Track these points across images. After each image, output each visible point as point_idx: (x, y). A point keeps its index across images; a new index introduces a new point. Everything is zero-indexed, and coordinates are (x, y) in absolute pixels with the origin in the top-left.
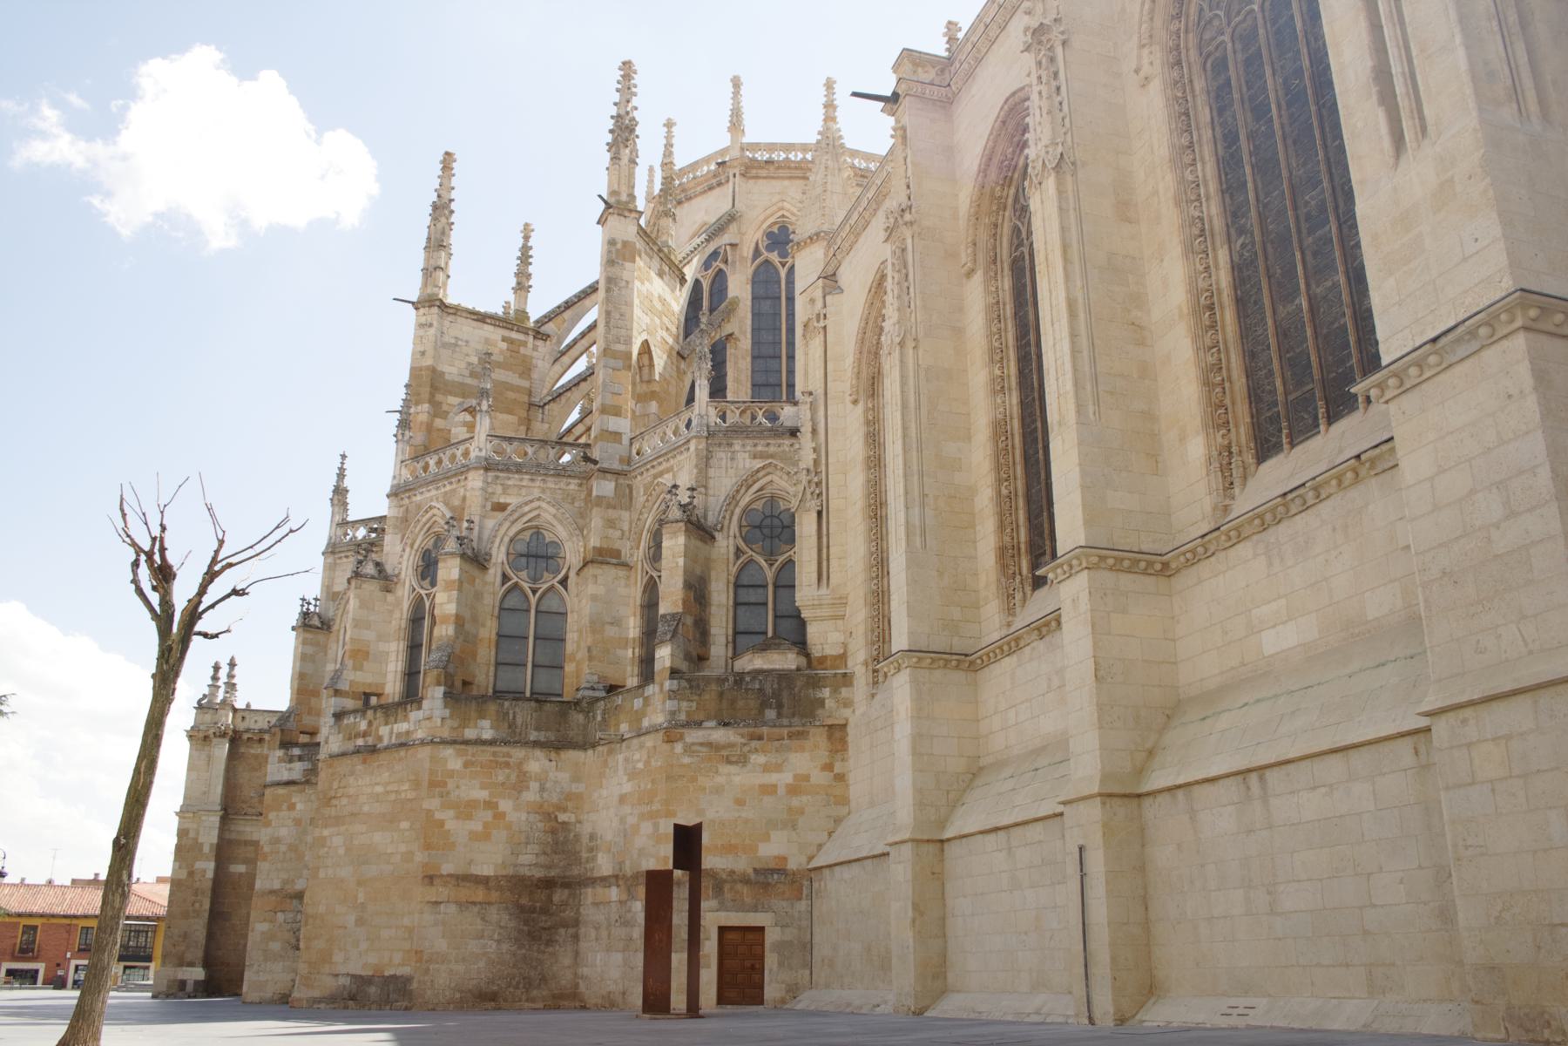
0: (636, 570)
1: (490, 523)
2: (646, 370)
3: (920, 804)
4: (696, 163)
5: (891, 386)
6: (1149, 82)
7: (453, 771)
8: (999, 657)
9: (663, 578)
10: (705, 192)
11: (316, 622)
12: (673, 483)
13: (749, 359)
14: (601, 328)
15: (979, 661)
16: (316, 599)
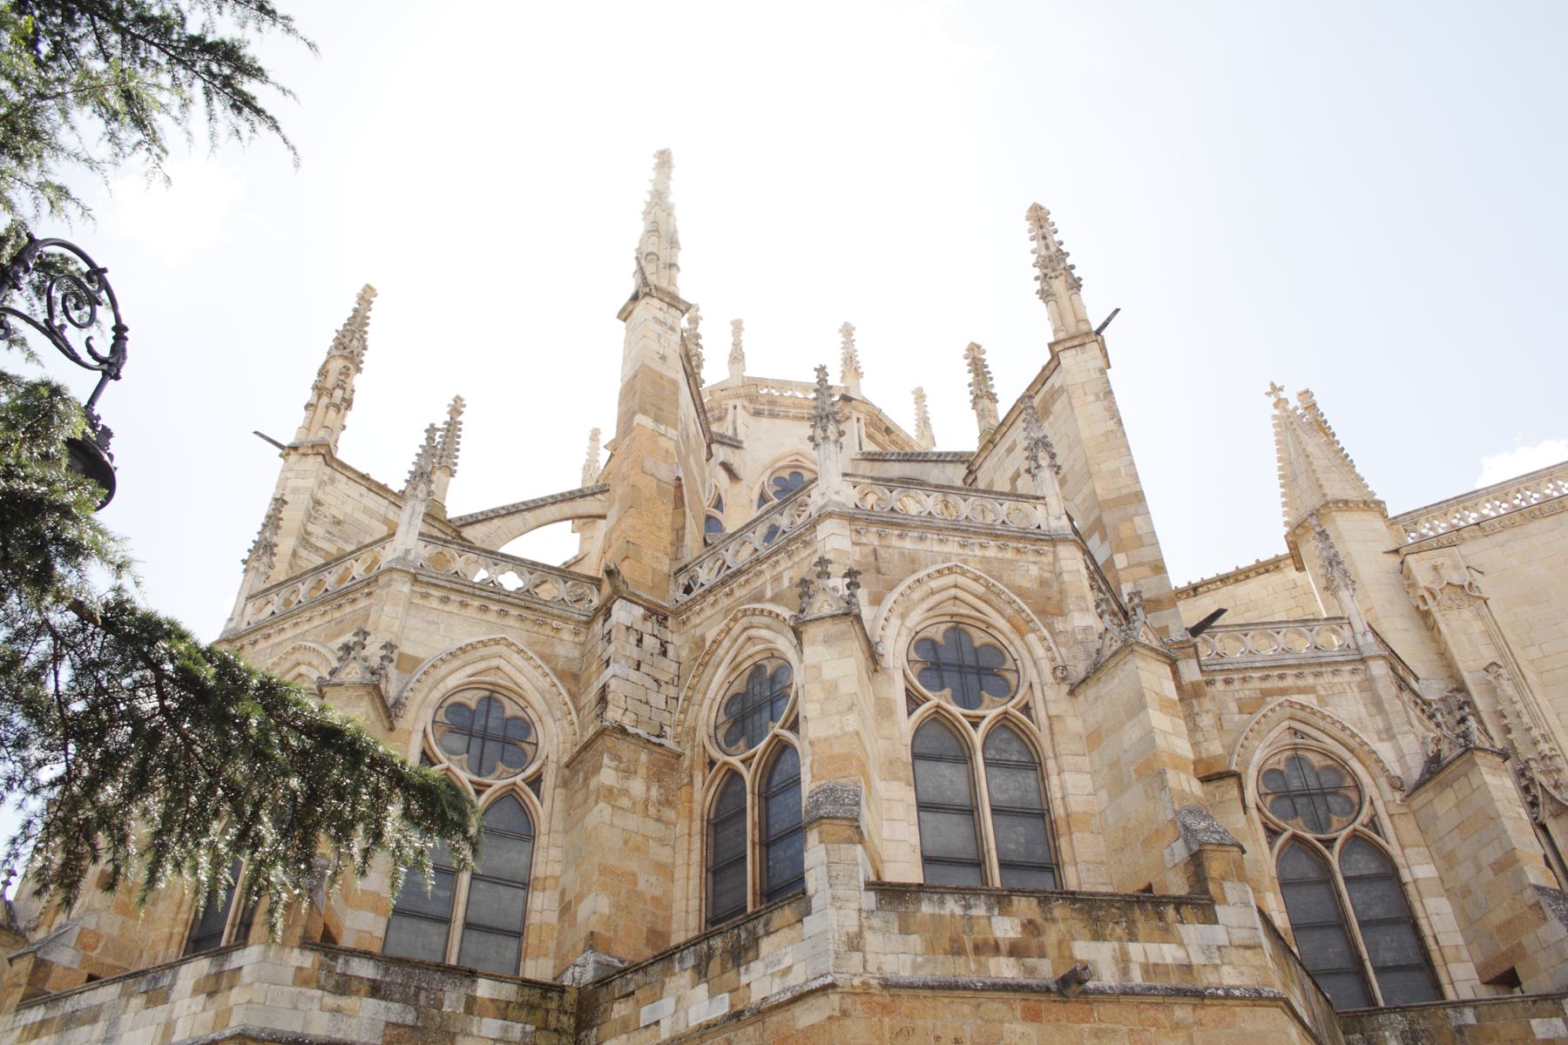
4: (790, 383)
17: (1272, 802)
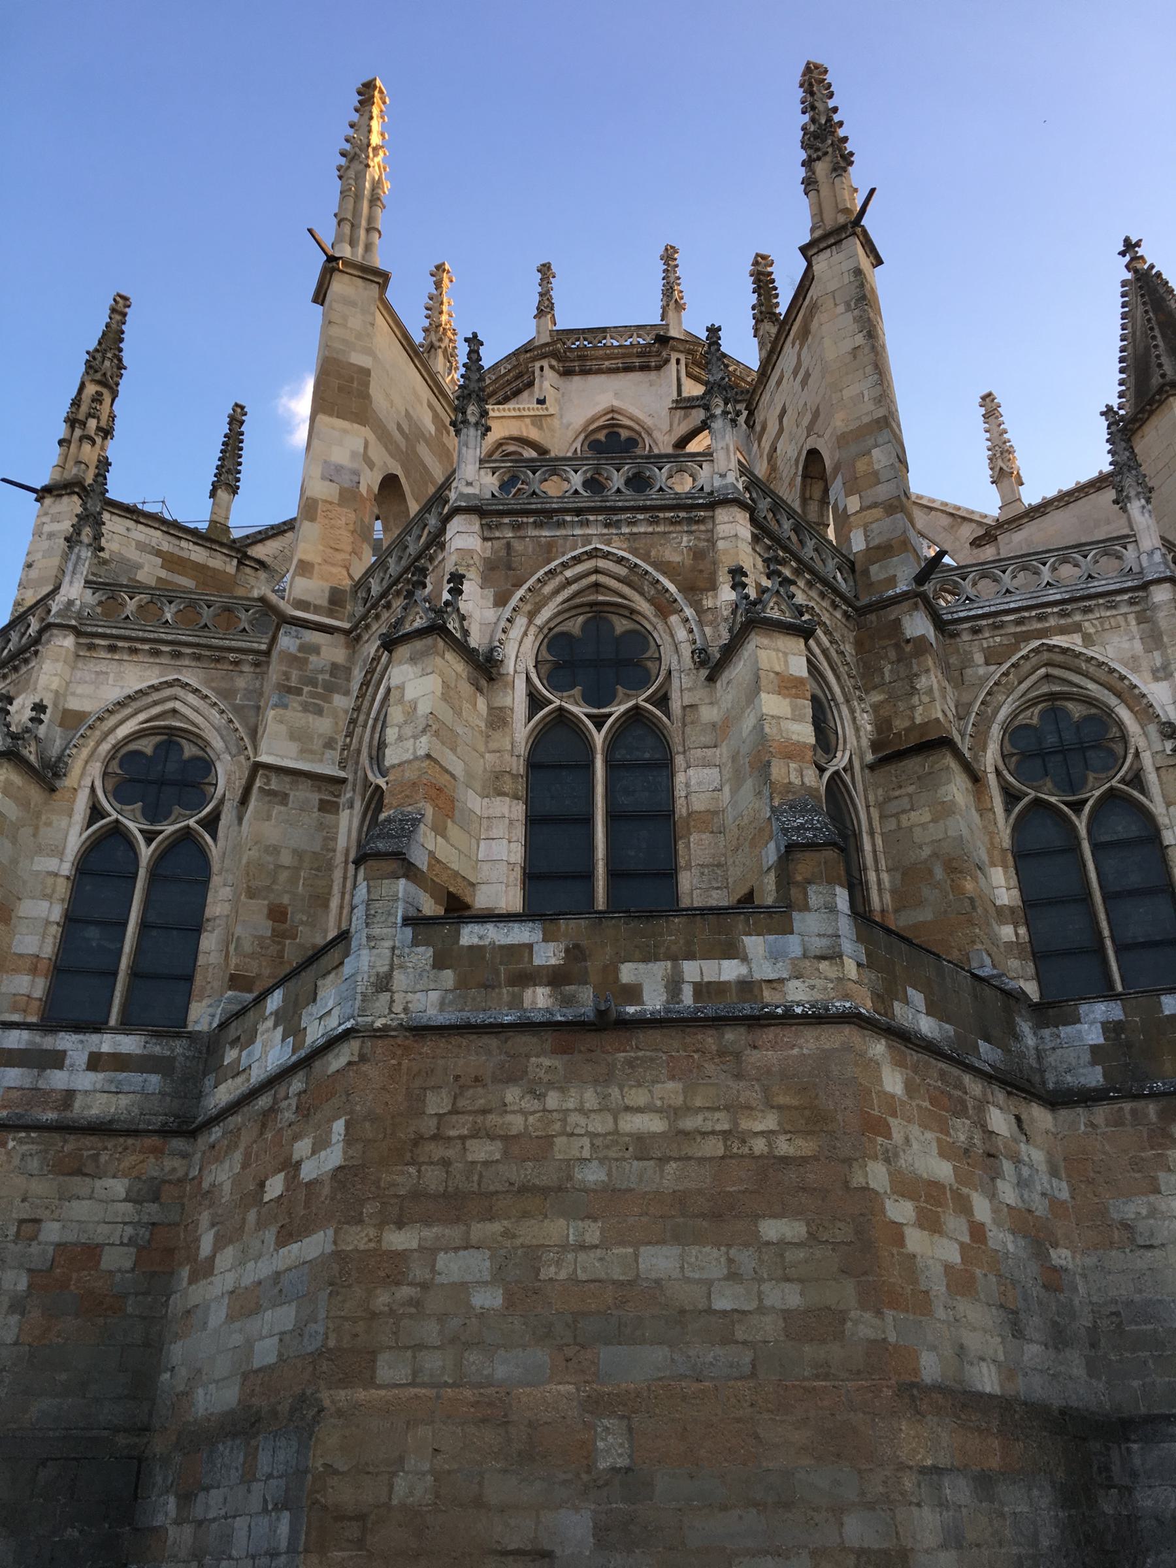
4: (604, 330)
17: (1018, 763)
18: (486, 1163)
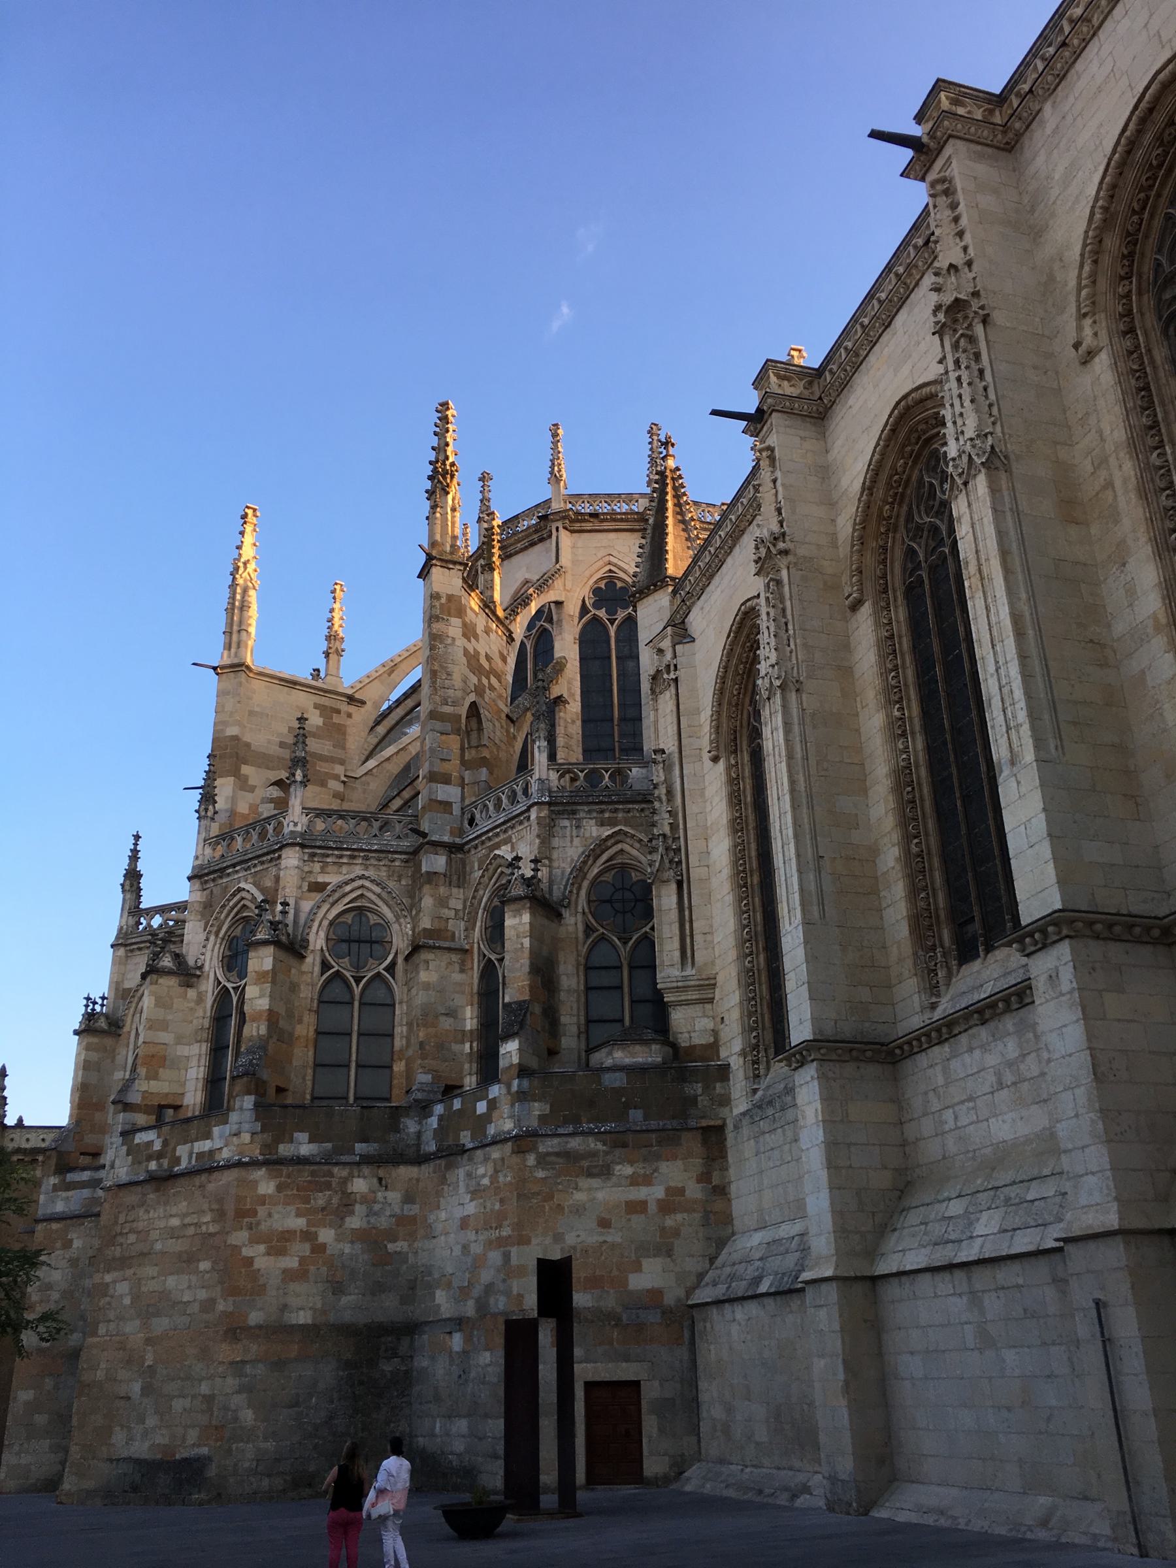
0: (472, 953)
1: (306, 906)
2: (474, 735)
3: (842, 1231)
4: (516, 517)
5: (773, 738)
6: (1093, 358)
7: (265, 1195)
8: (925, 1046)
9: (506, 962)
10: (526, 548)
11: (102, 1024)
12: (514, 854)
13: (579, 723)
14: (425, 690)
15: (898, 1051)
16: (103, 998)
18: (132, 1244)
